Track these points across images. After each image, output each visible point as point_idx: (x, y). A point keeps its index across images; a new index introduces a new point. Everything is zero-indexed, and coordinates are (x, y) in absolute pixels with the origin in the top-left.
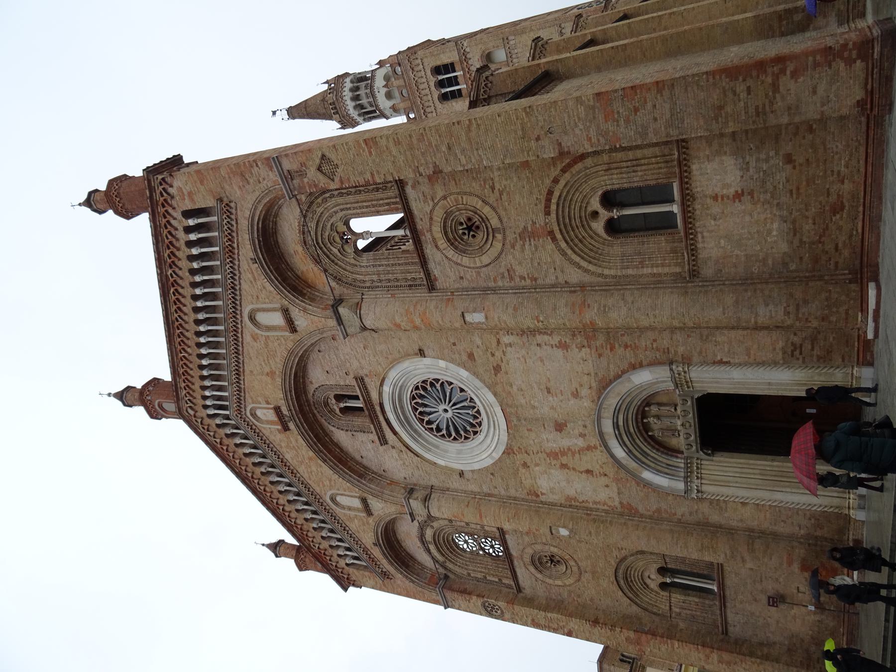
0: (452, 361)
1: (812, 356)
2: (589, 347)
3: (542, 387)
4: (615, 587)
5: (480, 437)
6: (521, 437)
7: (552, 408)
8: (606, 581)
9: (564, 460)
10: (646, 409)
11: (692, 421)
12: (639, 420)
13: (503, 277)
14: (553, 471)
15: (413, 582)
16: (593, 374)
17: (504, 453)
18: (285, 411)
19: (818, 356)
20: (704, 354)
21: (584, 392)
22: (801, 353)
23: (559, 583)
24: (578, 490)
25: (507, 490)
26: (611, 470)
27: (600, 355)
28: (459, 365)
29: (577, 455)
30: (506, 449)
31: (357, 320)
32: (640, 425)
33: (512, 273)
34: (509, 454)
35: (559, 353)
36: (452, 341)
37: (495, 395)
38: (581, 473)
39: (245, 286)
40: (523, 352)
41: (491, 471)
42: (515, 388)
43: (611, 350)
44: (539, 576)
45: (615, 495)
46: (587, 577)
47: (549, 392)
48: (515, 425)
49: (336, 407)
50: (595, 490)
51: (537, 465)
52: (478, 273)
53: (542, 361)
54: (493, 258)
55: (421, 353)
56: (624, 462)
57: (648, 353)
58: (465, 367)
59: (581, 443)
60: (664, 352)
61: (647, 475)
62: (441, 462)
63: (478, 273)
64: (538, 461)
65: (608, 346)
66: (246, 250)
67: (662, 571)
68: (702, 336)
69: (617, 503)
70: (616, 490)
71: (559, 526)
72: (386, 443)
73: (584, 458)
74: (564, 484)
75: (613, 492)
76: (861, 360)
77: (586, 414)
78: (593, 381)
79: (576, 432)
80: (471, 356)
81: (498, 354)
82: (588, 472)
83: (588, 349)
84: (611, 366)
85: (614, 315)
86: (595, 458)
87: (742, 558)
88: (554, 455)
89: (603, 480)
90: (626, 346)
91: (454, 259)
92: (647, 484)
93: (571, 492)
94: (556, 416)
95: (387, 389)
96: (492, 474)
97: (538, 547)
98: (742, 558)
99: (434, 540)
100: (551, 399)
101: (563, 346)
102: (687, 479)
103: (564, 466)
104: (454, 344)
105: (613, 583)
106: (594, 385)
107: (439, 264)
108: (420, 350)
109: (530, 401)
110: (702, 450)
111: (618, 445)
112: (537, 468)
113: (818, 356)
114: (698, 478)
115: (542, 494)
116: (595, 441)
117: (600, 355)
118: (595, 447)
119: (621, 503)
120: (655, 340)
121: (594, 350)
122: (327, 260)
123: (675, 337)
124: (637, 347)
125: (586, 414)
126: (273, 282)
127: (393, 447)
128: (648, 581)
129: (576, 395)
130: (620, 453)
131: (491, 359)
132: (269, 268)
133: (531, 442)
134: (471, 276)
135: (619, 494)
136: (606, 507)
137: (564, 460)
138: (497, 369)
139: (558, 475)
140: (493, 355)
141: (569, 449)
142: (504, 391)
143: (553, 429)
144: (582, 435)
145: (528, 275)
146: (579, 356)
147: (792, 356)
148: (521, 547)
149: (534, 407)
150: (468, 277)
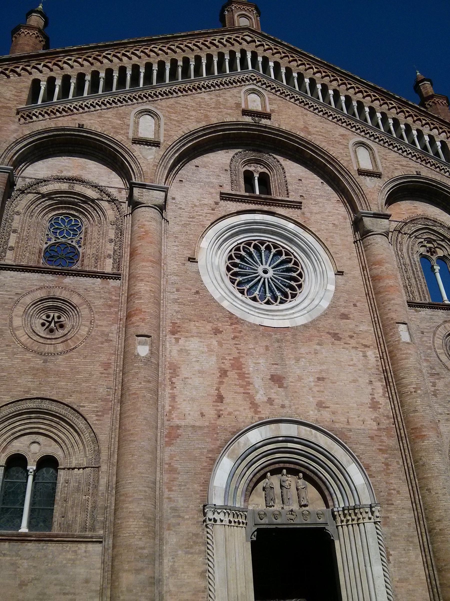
0: (336, 298)
2: (379, 429)
3: (324, 375)
4: (18, 394)
5: (239, 295)
6: (256, 337)
7: (300, 379)
8: (29, 384)
9: (232, 374)
10: (301, 475)
11: (297, 521)
12: (287, 465)
13: (432, 368)
14: (214, 358)
15: (17, 143)
16: (349, 427)
17: (230, 313)
18: (264, 122)
20: (393, 538)
23: (17, 322)
24: (189, 381)
25: (175, 301)
27: (372, 438)
28: (333, 302)
29: (242, 390)
30: (237, 318)
31: (380, 231)
32: (282, 465)
33: (436, 377)
34: (230, 318)
35: (367, 400)
36: (358, 304)
37: (305, 326)
38: (218, 389)
39: (393, 155)
40: (361, 366)
41: (201, 291)
42: (318, 347)
43: (380, 450)
44: (28, 300)
45: (189, 421)
46: (38, 362)
47: (319, 379)
48: (270, 336)
49: (257, 170)
50: (193, 400)
51: (220, 344)
52: (430, 348)
53: (355, 381)
54: (446, 364)
55: (340, 273)
57: (384, 484)
58: (330, 307)
59: (260, 397)
60: (388, 500)
61: (226, 465)
62: (205, 243)
63: (430, 348)
64: (225, 346)
65: (383, 448)
66: (427, 172)
67: (48, 462)
68: (412, 537)
69: (177, 422)
70: (197, 424)
71: (151, 346)
72: (222, 198)
73: (240, 397)
74: (197, 367)
75: (193, 418)
78: (342, 426)
79: (273, 396)
80: (345, 316)
81: (353, 342)
82: (220, 398)
83: (376, 427)
84: (362, 447)
85: (437, 458)
86: (241, 409)
87: (142, 569)
88: (237, 365)
89: (211, 413)
90: (387, 465)
91: (438, 332)
92: (213, 462)
93: (184, 372)
94: (291, 380)
95: (291, 226)
96: (197, 292)
97: (84, 311)
98: (142, 569)
99: (75, 194)
100: (311, 379)
101: (374, 405)
102: (226, 509)
103: (224, 373)
104: (355, 305)
105: (27, 392)
106: (337, 426)
107: (431, 319)
108: (343, 272)
109: (304, 358)
110: (258, 530)
112: (216, 343)
115: (177, 340)
116: (266, 413)
117: (372, 438)
118: (256, 412)
119: (178, 427)
120: (398, 492)
121: (376, 432)
122: (414, 229)
123: (405, 511)
124: (388, 474)
125: (298, 411)
126: (401, 178)
127: (217, 203)
128: (26, 440)
129: (321, 405)
130: (255, 437)
131: (347, 334)
132: (412, 181)
133: (251, 346)
134: (426, 341)
135: (193, 427)
136: (167, 408)
137: (232, 374)
138: (336, 336)
139: (211, 363)
140: (351, 337)
141: (249, 383)
142: (312, 336)
143: (273, 372)
144: (270, 401)
145: (438, 390)
148: (81, 292)
149: (297, 360)
150: (425, 339)
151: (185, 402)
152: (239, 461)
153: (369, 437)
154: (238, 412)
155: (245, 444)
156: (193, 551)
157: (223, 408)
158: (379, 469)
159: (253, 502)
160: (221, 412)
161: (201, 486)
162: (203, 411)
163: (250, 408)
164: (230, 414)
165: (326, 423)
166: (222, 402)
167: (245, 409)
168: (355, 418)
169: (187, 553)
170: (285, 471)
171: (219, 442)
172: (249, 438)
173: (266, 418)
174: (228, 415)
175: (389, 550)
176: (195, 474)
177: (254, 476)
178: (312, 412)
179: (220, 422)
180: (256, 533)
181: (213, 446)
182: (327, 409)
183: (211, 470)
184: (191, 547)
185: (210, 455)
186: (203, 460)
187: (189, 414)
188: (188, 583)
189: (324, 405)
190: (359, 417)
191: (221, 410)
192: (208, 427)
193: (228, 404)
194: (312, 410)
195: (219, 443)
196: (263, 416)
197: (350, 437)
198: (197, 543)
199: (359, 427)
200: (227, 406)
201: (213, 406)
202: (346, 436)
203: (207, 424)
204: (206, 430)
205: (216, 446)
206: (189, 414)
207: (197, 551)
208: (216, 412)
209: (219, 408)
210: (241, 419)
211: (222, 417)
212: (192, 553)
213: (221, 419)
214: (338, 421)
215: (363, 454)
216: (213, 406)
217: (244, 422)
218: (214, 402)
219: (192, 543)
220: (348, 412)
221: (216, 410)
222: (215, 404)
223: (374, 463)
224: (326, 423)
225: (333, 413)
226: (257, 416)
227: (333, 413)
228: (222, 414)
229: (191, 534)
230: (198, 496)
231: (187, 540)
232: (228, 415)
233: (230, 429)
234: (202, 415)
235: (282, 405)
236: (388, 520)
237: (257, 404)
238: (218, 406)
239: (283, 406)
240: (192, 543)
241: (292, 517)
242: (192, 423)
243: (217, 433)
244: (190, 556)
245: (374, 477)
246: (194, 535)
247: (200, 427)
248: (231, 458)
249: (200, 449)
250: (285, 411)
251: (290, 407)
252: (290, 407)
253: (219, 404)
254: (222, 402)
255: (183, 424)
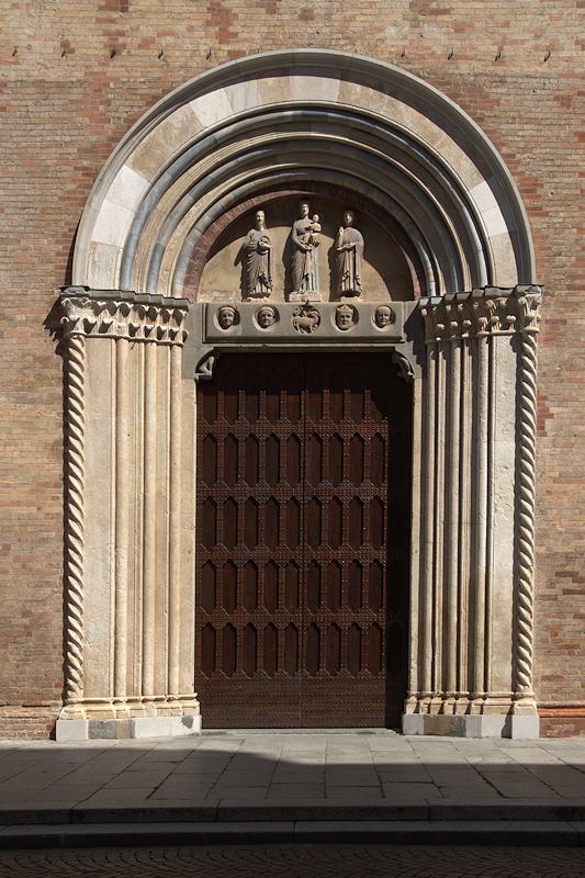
1: (560, 614)
16: (500, 70)
19: (560, 626)
20: (565, 374)
21: (437, 37)
22: (566, 592)
26: (134, 69)
45: (29, 68)
56: (177, 117)
70: (52, 75)
76: (552, 712)
77: (356, 26)
78: (479, 68)
84: (529, 130)
86: (180, 28)
89: (91, 43)
92: (90, 179)
111: (240, 110)
113: (560, 626)
114: (133, 331)
118: (225, 36)
130: (214, 109)
135: (40, 84)
146: (562, 39)
147: (558, 574)
151: (17, 12)
152: (167, 177)
153: (557, 98)
154: (170, 39)
155: (184, 130)
156: (36, 395)
157: (127, 27)
158: (565, 192)
159: (213, 287)
160: (121, 40)
161: (57, 242)
162: (71, 38)
163: (208, 23)
164: (145, 44)
165: (431, 61)
166: (124, 10)
167: (191, 29)
168: (523, 42)
169: (21, 400)
170: (306, 208)
171: (112, 126)
172: (197, 114)
173: (253, 52)
174: (140, 46)
175: (547, 403)
176: (43, 212)
177: (217, 217)
178: (391, 31)
179: (115, 69)
180: (212, 360)
181: (94, 138)
182: (440, 18)
183: (84, 201)
184: (31, 388)
185: (85, 163)
186: (65, 175)
187: (29, 47)
188: (22, 466)
189: (434, 5)
190: (537, 37)
191: (121, 34)
192: (81, 83)
193: (143, 14)
194: (395, 24)
195: (110, 128)
196: (245, 47)
197: (498, 102)
198: (46, 378)
199: (531, 70)
200: (139, 21)
201: (99, 21)
202: (485, 97)
203: (79, 75)
204: (76, 94)
205: (103, 139)
206: (29, 47)
207: (45, 395)
208: (105, 39)
209: (114, 28)
210: (177, 58)
211: (125, 53)
212: (32, 402)
213: (118, 61)
214: (468, 53)
215: (525, 150)
216: (99, 21)
217: (185, 67)
218: (101, 8)
219: (31, 379)
220: (506, 24)
221: (106, 33)
222: (105, 15)
223: (552, 174)
224: (431, 61)
225: (459, 29)
226: (226, 48)
227: (459, 29)
228: (124, 46)
229: (30, 358)
230: (51, 267)
231: (20, 370)
232: (140, 46)
233: (144, 90)
234: (66, 50)
235: (304, 10)
236: (562, 328)
237: (228, 11)
238: (113, 21)
239: (307, 16)
240: (31, 379)
241: (306, 320)
242: (36, 74)
243: (108, 103)
244: (26, 407)
245: (546, 214)
246: (37, 359)
247: (59, 85)
248: (141, 169)
249: (59, 145)
250: (311, 27)
251: (328, 16)
252: (328, 16)
253: (115, 15)
254: (124, 10)
255: (13, 76)
